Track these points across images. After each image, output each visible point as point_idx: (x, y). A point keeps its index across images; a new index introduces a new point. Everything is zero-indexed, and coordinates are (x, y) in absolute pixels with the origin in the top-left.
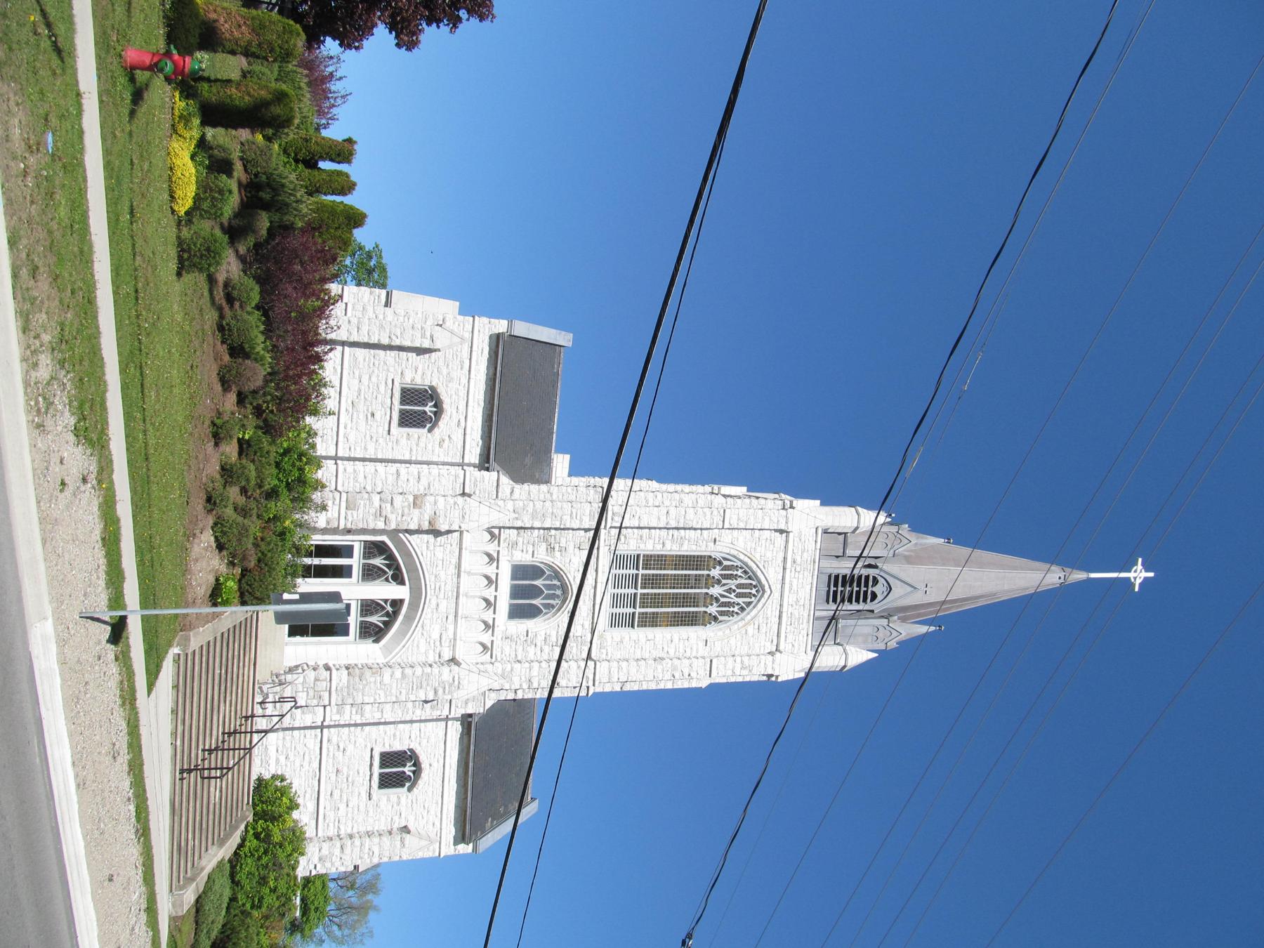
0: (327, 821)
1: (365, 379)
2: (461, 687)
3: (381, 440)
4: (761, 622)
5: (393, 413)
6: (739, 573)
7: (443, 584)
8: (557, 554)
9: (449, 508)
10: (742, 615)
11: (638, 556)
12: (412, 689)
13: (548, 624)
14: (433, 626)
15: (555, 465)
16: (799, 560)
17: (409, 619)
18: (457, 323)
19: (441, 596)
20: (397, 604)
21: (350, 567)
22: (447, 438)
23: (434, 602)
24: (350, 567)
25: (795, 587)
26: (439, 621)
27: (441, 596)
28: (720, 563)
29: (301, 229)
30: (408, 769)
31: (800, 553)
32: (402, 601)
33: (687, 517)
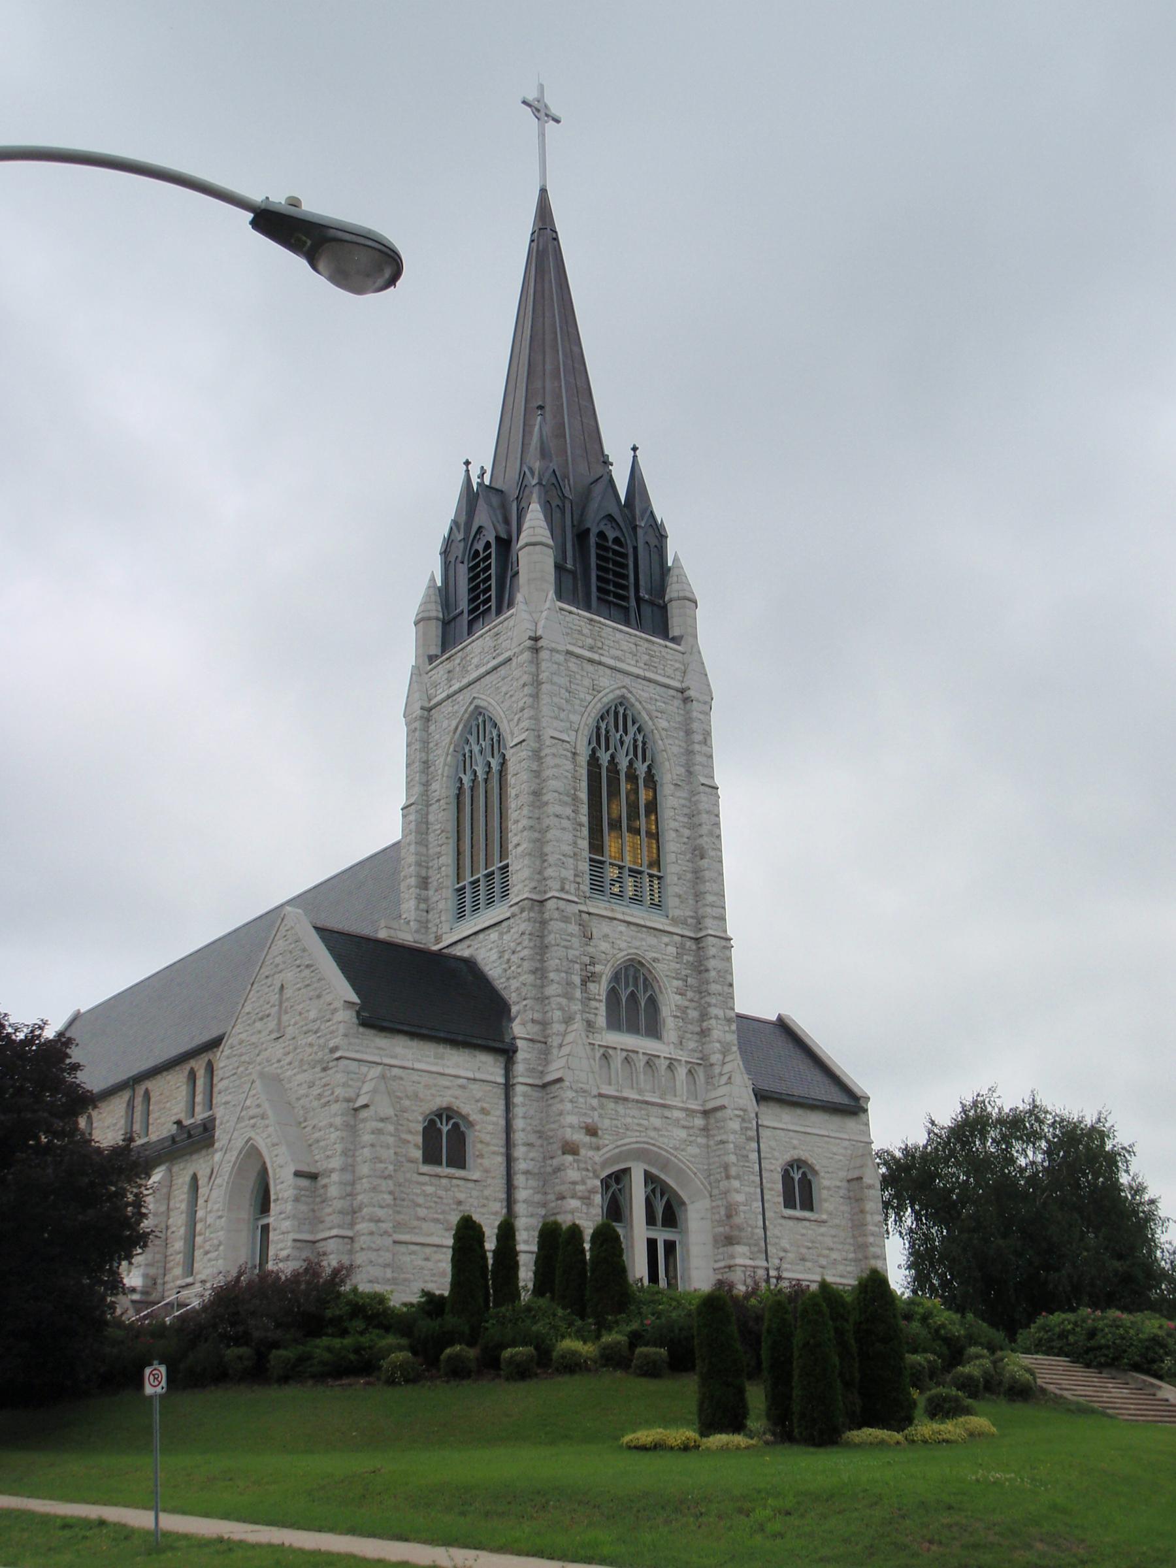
0: (845, 1273)
1: (422, 1212)
2: (745, 1107)
3: (486, 1193)
4: (654, 708)
5: (457, 1175)
6: (603, 726)
7: (636, 1121)
8: (598, 968)
9: (576, 1110)
10: (647, 730)
11: (591, 860)
12: (748, 1167)
13: (666, 989)
14: (675, 1137)
15: (401, 941)
16: (590, 641)
17: (665, 1165)
18: (350, 1083)
19: (645, 1122)
20: (649, 1178)
21: (666, 1242)
22: (479, 1104)
23: (653, 1134)
24: (666, 1242)
25: (619, 653)
26: (670, 1128)
27: (645, 1122)
28: (594, 751)
29: (560, 1317)
30: (797, 1176)
31: (583, 638)
32: (646, 1172)
33: (561, 790)
